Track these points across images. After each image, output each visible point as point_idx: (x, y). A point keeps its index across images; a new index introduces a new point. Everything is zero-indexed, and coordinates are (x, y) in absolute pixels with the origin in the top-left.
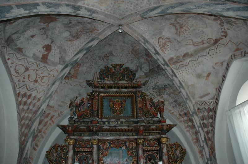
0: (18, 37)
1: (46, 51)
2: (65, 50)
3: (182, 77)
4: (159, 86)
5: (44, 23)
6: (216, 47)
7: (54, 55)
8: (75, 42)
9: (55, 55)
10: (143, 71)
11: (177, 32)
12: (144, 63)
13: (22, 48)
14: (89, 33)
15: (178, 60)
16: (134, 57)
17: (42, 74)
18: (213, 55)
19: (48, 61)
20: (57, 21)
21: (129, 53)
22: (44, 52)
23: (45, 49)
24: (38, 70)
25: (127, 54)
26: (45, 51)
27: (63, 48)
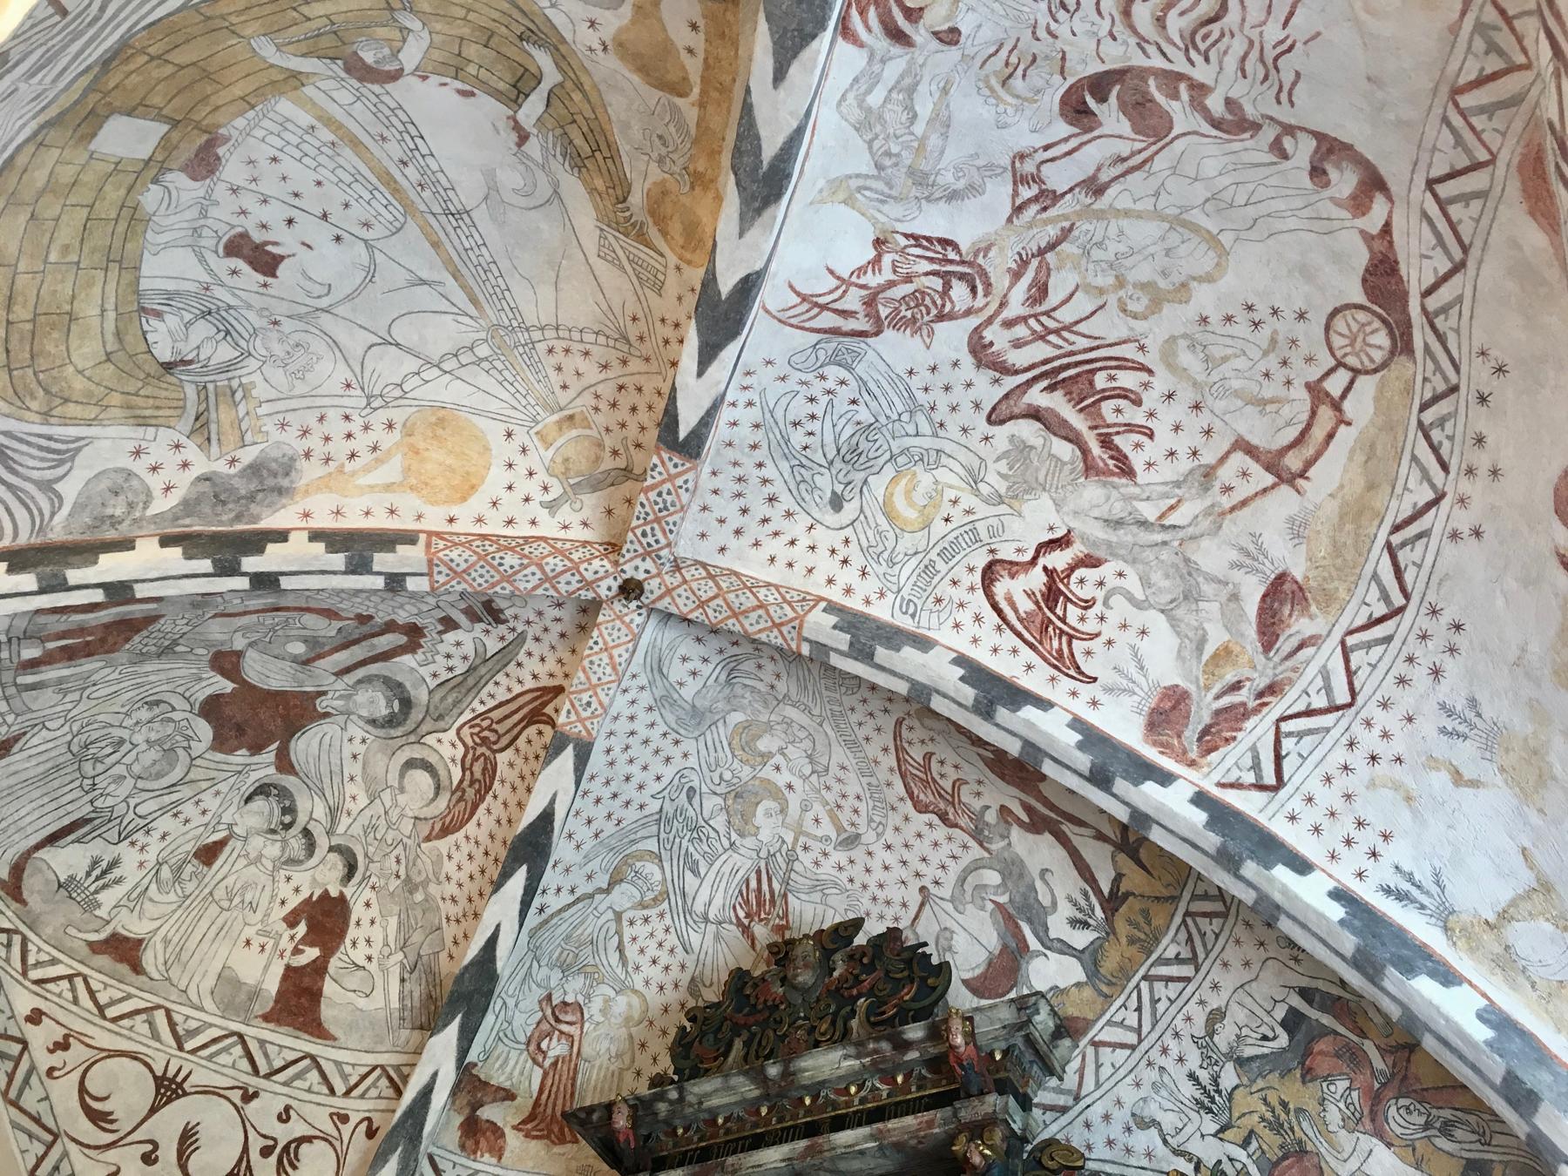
0: (95, 863)
1: (312, 945)
5: (256, 749)
6: (1436, 347)
7: (362, 962)
10: (1065, 948)
11: (1085, 452)
13: (140, 941)
15: (1236, 687)
17: (284, 1117)
18: (1480, 440)
20: (327, 715)
22: (297, 951)
23: (302, 929)
24: (256, 1095)
26: (303, 940)
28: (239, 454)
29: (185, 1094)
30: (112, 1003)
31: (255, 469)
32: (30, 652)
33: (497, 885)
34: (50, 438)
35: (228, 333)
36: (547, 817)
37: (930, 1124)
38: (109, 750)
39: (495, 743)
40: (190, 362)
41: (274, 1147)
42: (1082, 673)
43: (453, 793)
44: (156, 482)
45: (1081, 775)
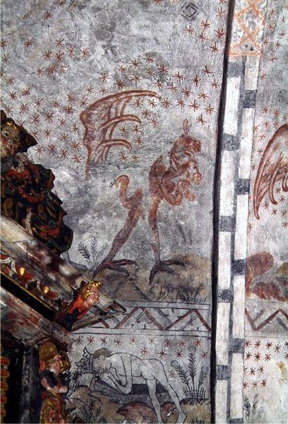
3: (254, 378)
4: (105, 377)
12: (105, 210)
16: (75, 146)
21: (69, 111)
25: (56, 104)
37: (36, 321)
42: (257, 210)
45: (232, 256)
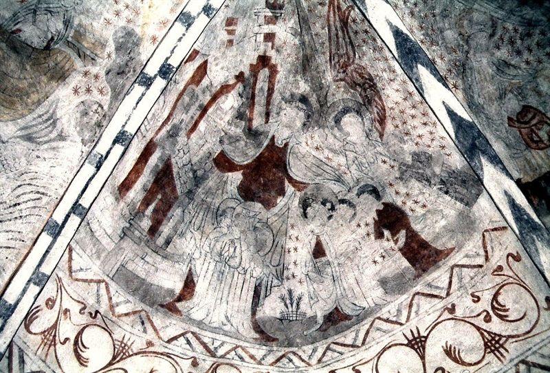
0: (283, 299)
1: (398, 232)
2: (416, 156)
5: (282, 192)
8: (389, 104)
9: (424, 206)
13: (336, 308)
14: (352, 34)
17: (477, 299)
19: (438, 245)
20: (286, 145)
23: (387, 233)
24: (453, 306)
26: (393, 235)
27: (409, 160)
28: (108, 50)
29: (426, 338)
30: (355, 340)
31: (119, 48)
32: (146, 223)
33: (420, 91)
34: (40, 116)
35: (51, 12)
36: (397, 33)
38: (232, 250)
39: (349, 59)
40: (52, 38)
41: (488, 313)
43: (365, 105)
44: (96, 96)
